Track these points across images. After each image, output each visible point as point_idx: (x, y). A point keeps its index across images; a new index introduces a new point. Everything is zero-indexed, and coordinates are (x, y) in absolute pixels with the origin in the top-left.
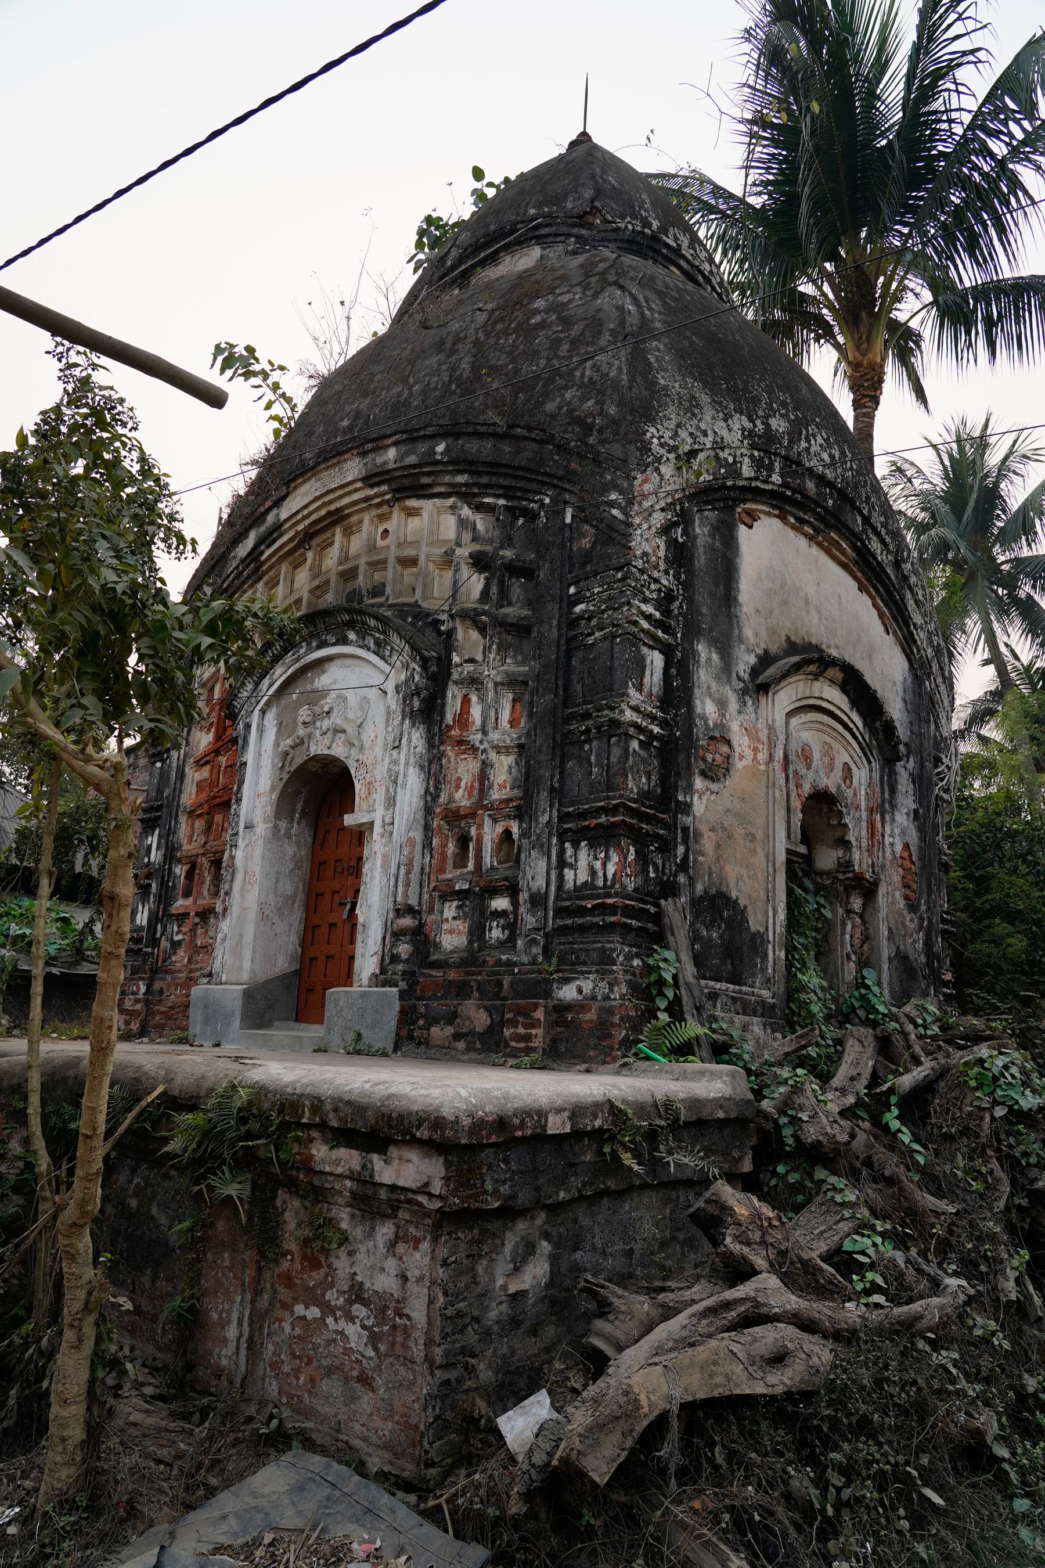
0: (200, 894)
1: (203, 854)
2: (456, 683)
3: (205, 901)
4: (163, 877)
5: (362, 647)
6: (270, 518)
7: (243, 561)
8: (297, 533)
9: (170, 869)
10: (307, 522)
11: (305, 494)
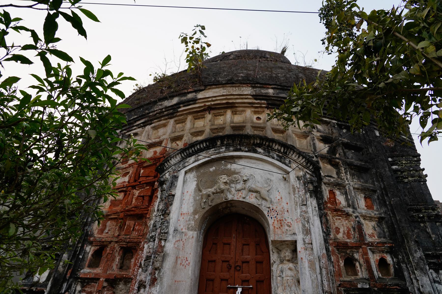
0: (111, 267)
1: (116, 242)
2: (325, 184)
3: (115, 270)
4: (75, 251)
5: (269, 156)
6: (190, 96)
7: (166, 107)
8: (205, 105)
9: (82, 247)
10: (213, 103)
11: (216, 92)
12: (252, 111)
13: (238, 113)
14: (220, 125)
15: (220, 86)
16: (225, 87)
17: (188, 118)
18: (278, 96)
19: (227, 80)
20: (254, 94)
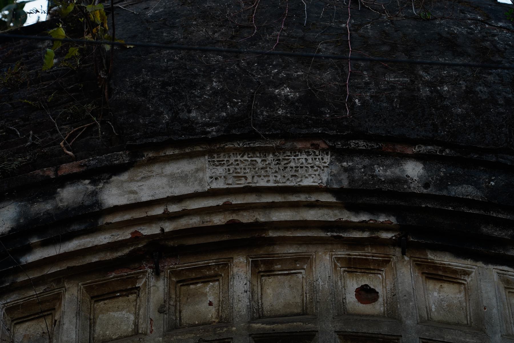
8: (137, 238)
10: (169, 227)
11: (184, 178)
12: (338, 259)
13: (279, 267)
14: (206, 324)
15: (199, 149)
16: (218, 153)
17: (67, 296)
18: (445, 193)
19: (225, 120)
20: (345, 184)
